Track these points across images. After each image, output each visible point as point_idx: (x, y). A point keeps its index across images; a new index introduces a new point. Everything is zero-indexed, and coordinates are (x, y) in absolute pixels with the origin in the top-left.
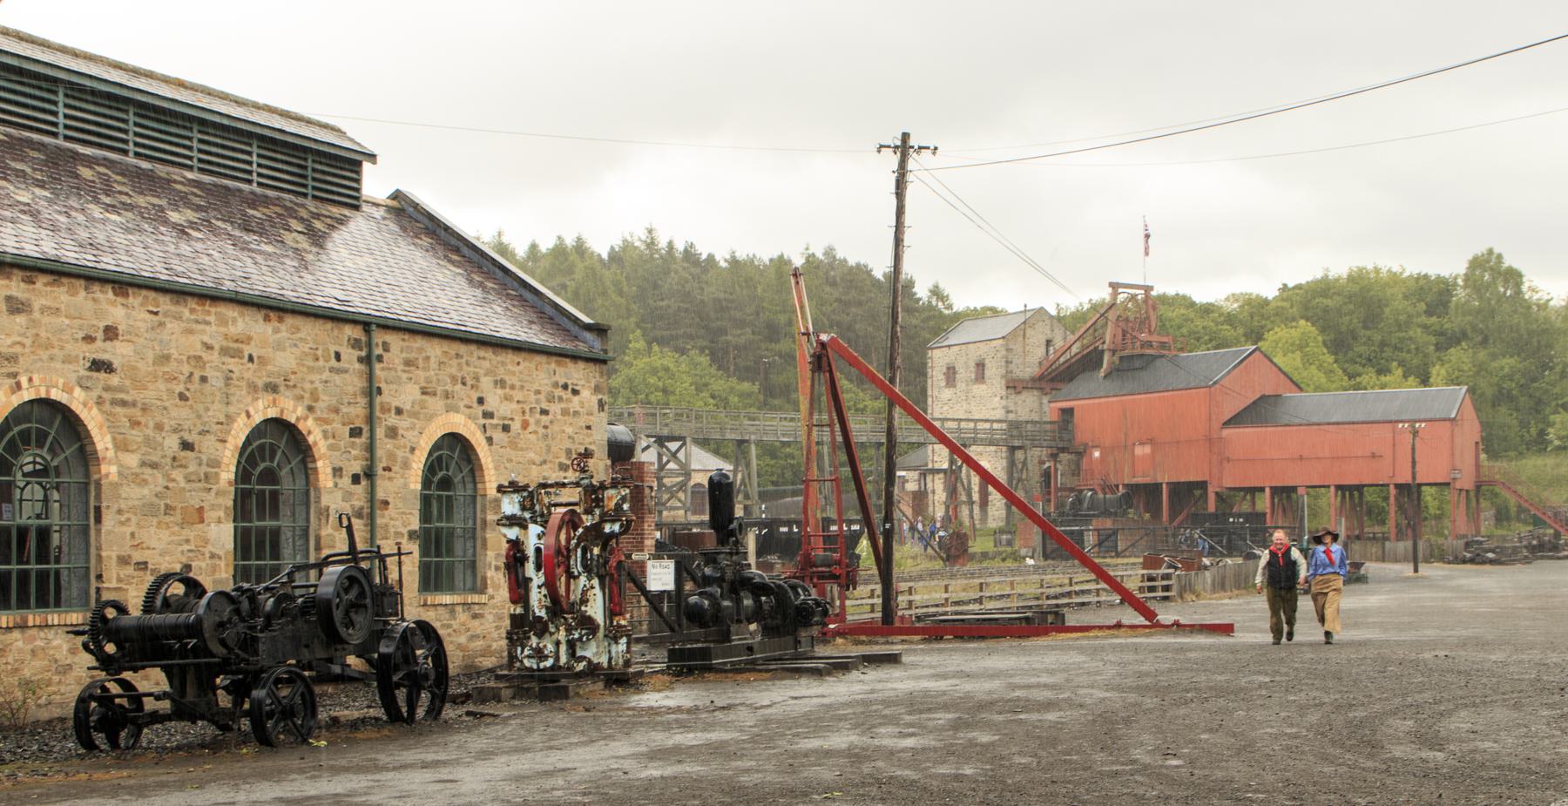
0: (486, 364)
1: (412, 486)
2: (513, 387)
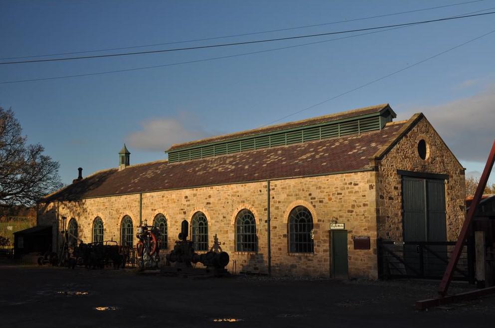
1: (284, 222)
2: (324, 188)
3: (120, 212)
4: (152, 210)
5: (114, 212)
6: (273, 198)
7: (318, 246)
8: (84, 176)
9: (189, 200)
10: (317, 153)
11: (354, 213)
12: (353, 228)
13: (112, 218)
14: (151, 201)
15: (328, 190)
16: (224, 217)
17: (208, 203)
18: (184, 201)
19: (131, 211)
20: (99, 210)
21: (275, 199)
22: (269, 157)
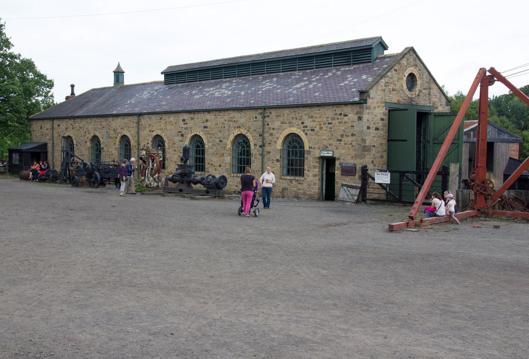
0: (306, 112)
3: (118, 131)
4: (150, 131)
5: (112, 132)
6: (268, 124)
7: (308, 171)
8: (77, 93)
9: (187, 124)
10: (311, 82)
11: (342, 142)
12: (341, 156)
13: (110, 138)
14: (150, 123)
15: (319, 120)
16: (221, 141)
17: (205, 127)
18: (181, 124)
19: (129, 131)
20: (95, 129)
21: (270, 126)
22: (264, 84)
